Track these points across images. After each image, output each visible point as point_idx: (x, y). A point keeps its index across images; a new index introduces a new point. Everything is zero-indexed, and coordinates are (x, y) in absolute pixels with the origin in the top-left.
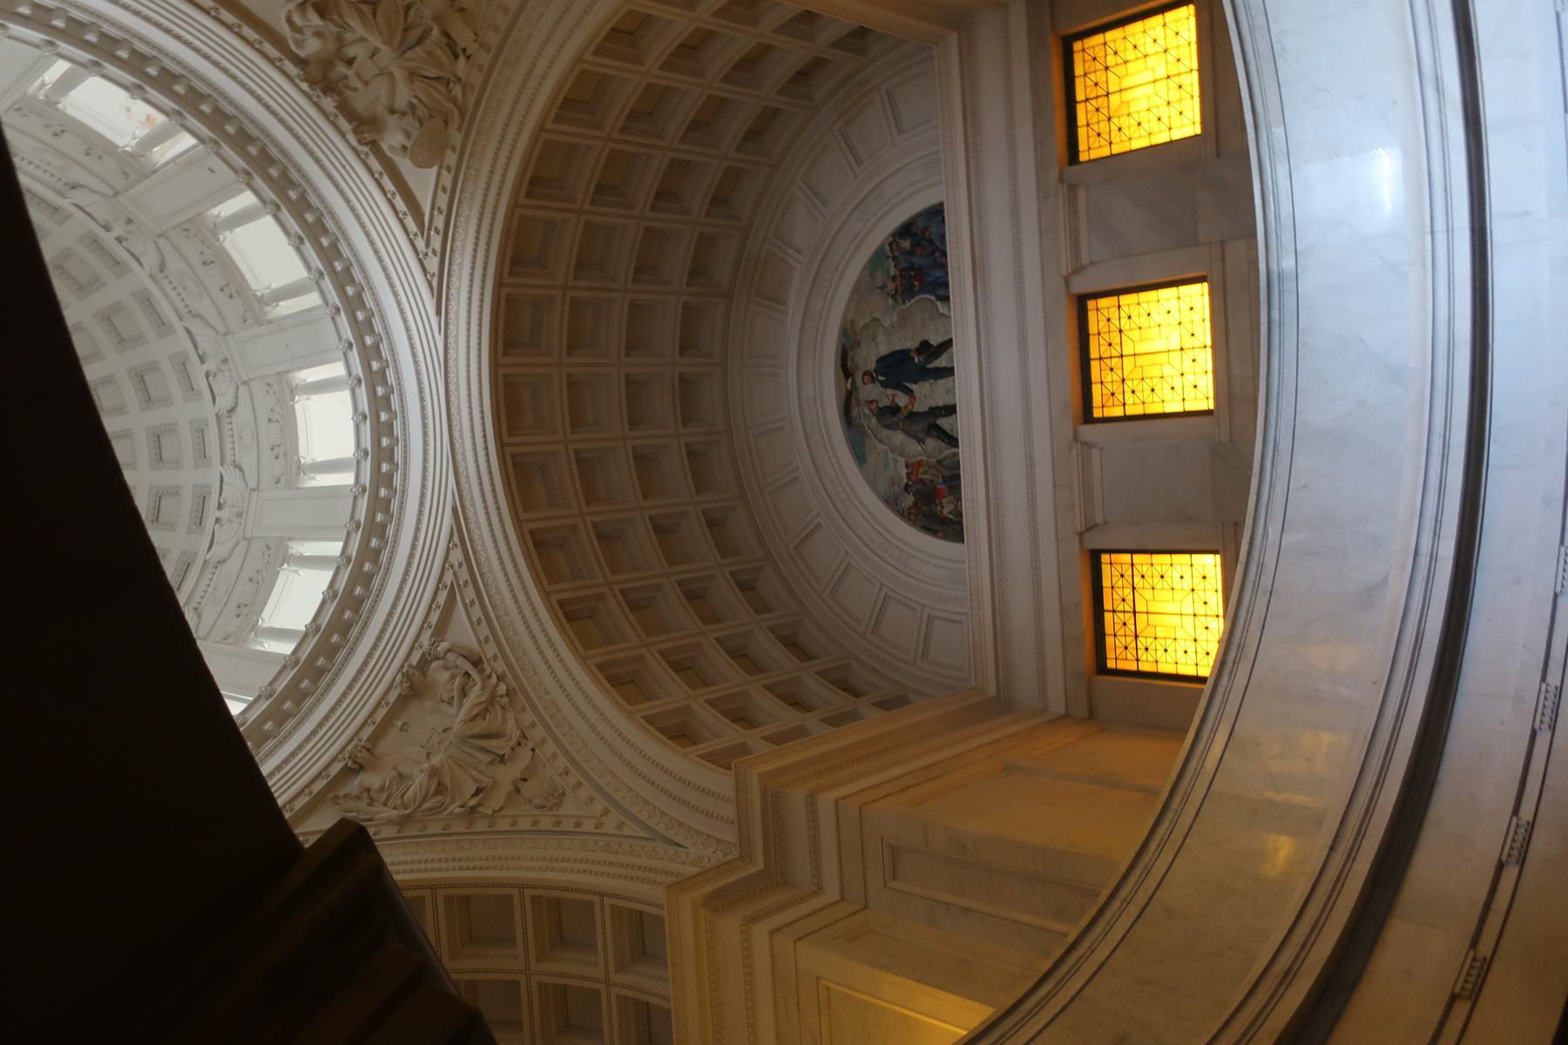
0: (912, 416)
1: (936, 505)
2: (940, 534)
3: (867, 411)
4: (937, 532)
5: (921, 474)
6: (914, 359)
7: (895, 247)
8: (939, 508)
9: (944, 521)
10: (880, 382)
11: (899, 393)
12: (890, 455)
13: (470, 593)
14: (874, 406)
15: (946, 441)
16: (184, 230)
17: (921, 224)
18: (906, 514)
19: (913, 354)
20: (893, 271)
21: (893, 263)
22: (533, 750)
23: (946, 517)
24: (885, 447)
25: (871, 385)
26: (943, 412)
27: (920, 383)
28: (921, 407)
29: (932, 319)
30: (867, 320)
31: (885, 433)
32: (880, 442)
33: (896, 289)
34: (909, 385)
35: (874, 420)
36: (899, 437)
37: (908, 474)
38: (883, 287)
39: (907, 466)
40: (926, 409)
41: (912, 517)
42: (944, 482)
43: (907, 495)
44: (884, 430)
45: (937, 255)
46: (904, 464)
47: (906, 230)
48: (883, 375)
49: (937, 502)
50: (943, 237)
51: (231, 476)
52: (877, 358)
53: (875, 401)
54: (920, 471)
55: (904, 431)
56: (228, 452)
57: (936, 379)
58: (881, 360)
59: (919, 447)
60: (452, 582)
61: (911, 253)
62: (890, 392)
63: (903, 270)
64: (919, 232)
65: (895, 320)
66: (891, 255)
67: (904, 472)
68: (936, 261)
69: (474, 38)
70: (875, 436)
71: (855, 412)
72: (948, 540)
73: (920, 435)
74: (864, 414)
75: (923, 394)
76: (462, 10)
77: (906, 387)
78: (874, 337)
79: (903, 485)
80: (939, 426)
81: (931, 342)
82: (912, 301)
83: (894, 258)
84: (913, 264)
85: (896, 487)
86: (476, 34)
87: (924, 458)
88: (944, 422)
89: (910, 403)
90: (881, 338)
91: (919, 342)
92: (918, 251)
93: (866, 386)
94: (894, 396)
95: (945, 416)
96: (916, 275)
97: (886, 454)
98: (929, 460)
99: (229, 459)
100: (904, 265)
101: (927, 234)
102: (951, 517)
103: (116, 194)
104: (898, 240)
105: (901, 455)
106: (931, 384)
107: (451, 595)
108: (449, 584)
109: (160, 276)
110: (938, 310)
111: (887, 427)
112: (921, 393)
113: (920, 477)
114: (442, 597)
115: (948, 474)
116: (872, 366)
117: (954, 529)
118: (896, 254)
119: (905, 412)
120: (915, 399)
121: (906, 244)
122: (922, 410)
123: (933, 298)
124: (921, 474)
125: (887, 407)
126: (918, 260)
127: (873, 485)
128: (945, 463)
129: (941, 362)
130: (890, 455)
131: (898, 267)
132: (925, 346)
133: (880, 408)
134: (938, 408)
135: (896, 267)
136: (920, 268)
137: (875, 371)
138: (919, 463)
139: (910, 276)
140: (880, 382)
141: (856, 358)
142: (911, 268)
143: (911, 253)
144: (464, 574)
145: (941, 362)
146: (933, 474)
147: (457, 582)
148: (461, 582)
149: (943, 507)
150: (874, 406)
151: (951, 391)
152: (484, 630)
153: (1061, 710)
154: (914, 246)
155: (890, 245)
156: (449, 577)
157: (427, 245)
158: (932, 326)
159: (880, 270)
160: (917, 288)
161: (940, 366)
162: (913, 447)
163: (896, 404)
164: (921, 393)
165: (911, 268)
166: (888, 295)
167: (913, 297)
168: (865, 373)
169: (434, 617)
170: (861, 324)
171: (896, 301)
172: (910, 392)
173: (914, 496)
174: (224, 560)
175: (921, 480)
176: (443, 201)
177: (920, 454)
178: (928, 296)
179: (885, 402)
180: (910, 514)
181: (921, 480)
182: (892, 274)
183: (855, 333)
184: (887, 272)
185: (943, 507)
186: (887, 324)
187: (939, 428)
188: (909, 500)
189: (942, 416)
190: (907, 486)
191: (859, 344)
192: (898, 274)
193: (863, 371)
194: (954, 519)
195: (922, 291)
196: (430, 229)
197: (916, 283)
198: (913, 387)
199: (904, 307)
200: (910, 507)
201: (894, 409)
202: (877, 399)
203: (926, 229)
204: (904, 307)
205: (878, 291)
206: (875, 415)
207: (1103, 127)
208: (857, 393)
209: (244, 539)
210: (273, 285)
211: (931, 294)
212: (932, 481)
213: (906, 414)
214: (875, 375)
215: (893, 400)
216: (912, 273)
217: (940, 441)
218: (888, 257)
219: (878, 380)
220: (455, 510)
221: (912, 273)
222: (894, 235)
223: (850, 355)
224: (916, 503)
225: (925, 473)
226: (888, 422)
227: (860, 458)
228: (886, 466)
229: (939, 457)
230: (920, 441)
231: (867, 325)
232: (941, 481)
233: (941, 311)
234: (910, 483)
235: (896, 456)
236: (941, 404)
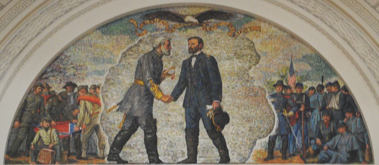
0: (150, 97)
1: (50, 121)
2: (17, 123)
4: (20, 121)
5: (85, 103)
6: (211, 103)
7: (333, 89)
8: (46, 124)
9: (31, 129)
10: (190, 60)
12: (110, 66)
14: (164, 49)
15: (118, 138)
17: (353, 124)
18: (43, 82)
19: (215, 103)
20: (308, 85)
21: (315, 86)
23: (35, 134)
24: (117, 62)
25: (187, 48)
26: (149, 136)
27: (183, 111)
30: (258, 47)
31: (134, 62)
32: (125, 55)
33: (288, 87)
34: (183, 96)
35: (149, 48)
37: (86, 87)
38: (292, 71)
39: (95, 87)
40: (155, 116)
41: (38, 90)
42: (74, 134)
43: (63, 84)
44: (136, 61)
45: (318, 141)
46: (97, 84)
48: (196, 63)
49: (53, 123)
52: (215, 58)
53: (169, 51)
54: (87, 102)
55: (134, 86)
57: (186, 130)
58: (213, 62)
59: (115, 104)
61: (323, 109)
62: (178, 71)
63: (307, 98)
64: (345, 120)
65: (255, 84)
66: (324, 84)
67: (89, 82)
68: (311, 139)
70: (130, 49)
71: (160, 24)
72: (11, 133)
73: (128, 106)
74: (154, 37)
75: (171, 113)
77: (181, 92)
78: (239, 56)
79: (74, 81)
80: (136, 130)
81: (226, 127)
82: (273, 107)
83: (321, 87)
84: (312, 110)
85: (72, 71)
88: (138, 137)
89: (164, 96)
90: (237, 64)
91: (228, 112)
92: (325, 118)
93: (186, 42)
95: (145, 139)
96: (300, 113)
97: (110, 61)
98: (100, 115)
100: (312, 99)
101: (341, 130)
102: (36, 138)
104: (339, 93)
105: (107, 80)
106: (181, 124)
110: (260, 138)
111: (140, 64)
112: (173, 110)
113: (82, 103)
115: (82, 138)
116: (208, 51)
117: (21, 142)
118: (325, 90)
120: (168, 102)
121: (334, 104)
122: (154, 110)
123: (273, 133)
124: (85, 103)
125: (162, 65)
126: (316, 116)
128: (95, 136)
129: (204, 140)
130: (110, 66)
131: (311, 92)
133: (161, 57)
134: (155, 130)
135: (312, 88)
136: (307, 119)
137: (202, 53)
138: (96, 103)
139: (299, 106)
140: (190, 60)
141: (219, 30)
142: (308, 109)
143: (323, 109)
145: (204, 140)
146: (83, 119)
149: (47, 130)
150: (164, 49)
154: (330, 113)
155: (336, 83)
158: (242, 129)
159: (310, 68)
160: (286, 114)
161: (200, 137)
163: (164, 78)
164: (173, 110)
165: (308, 109)
166: (283, 77)
167: (276, 109)
168: (201, 41)
170: (254, 40)
171: (275, 86)
172: (175, 96)
173: (60, 94)
175: (78, 104)
177: (106, 105)
178: (276, 126)
179: (167, 65)
180: (42, 86)
182: (304, 83)
183: (246, 31)
185: (47, 130)
187: (132, 130)
188: (57, 87)
189: (146, 134)
190: (74, 86)
191: (234, 36)
192: (303, 91)
193: (203, 39)
194: (32, 143)
195: (282, 117)
197: (291, 113)
198: (180, 101)
199: (267, 95)
200: (49, 88)
202: (171, 53)
203: (348, 130)
204: (267, 95)
205: (288, 64)
206: (154, 49)
208: (180, 29)
211: (276, 130)
212: (76, 118)
213: (151, 89)
214: (198, 53)
215: (168, 75)
216: (302, 109)
217: (119, 130)
218: (322, 81)
219: (192, 57)
221: (302, 109)
222: (345, 88)
223: (223, 23)
224: (52, 95)
225: (86, 108)
226: (145, 67)
228: (96, 60)
229: (101, 129)
231: (252, 47)
232: (76, 128)
233: (258, 141)
234: (76, 90)
235: (107, 73)
236: (158, 134)
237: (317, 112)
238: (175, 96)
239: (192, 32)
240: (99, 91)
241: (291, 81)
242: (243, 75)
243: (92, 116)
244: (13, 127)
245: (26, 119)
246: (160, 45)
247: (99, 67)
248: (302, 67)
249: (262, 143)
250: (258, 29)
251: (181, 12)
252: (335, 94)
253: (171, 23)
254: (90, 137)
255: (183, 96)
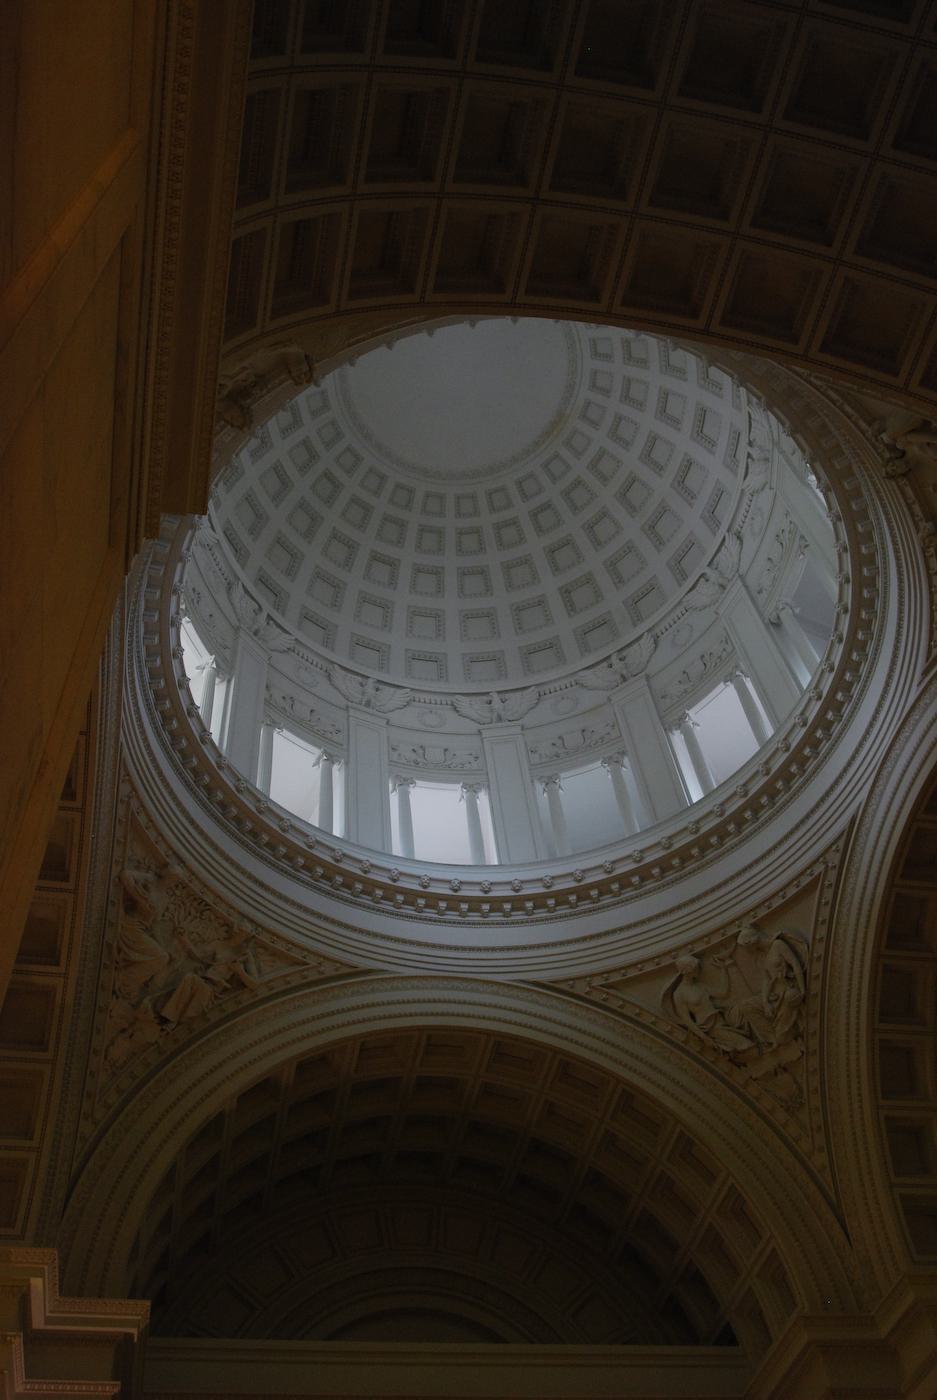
13: (296, 981)
16: (613, 726)
22: (156, 1042)
51: (399, 697)
56: (423, 696)
60: (307, 964)
69: (754, 1077)
76: (776, 1074)
86: (755, 1080)
99: (418, 696)
103: (648, 677)
107: (298, 963)
108: (308, 961)
109: (572, 680)
114: (296, 954)
144: (313, 976)
147: (308, 969)
148: (305, 973)
152: (264, 993)
156: (312, 961)
157: (593, 987)
169: (280, 946)
174: (330, 680)
176: (628, 1011)
196: (608, 993)
209: (347, 707)
210: (561, 791)
220: (369, 972)
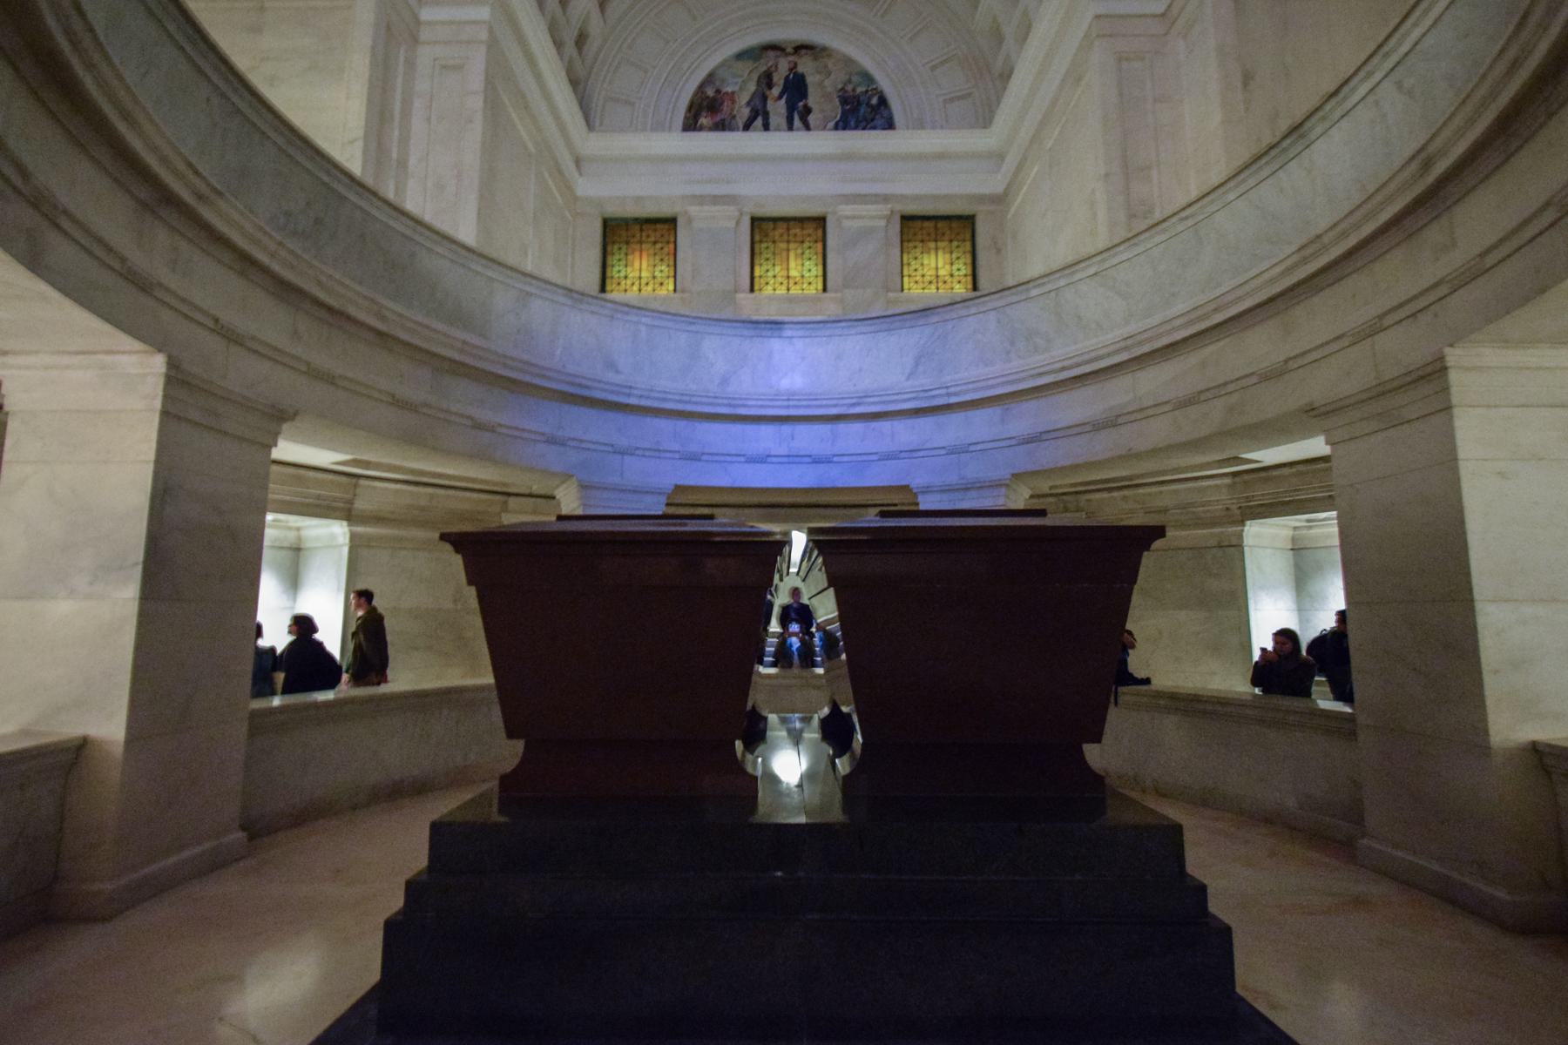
0: (765, 98)
2: (688, 115)
3: (770, 64)
9: (696, 117)
11: (781, 87)
12: (740, 80)
14: (773, 69)
17: (885, 114)
20: (860, 90)
28: (770, 105)
29: (824, 117)
31: (755, 77)
32: (751, 72)
33: (846, 91)
34: (785, 97)
35: (764, 68)
36: (752, 87)
39: (733, 93)
43: (714, 90)
47: (883, 101)
50: (874, 128)
55: (756, 90)
62: (782, 82)
63: (859, 98)
66: (870, 89)
67: (729, 89)
71: (771, 54)
74: (768, 61)
78: (819, 73)
83: (867, 91)
87: (737, 107)
88: (759, 122)
90: (818, 78)
92: (869, 110)
94: (779, 85)
97: (742, 76)
100: (861, 98)
111: (759, 78)
115: (727, 123)
116: (800, 69)
118: (870, 93)
119: (768, 93)
121: (874, 101)
126: (863, 110)
127: (722, 65)
129: (797, 122)
132: (808, 110)
138: (733, 102)
139: (853, 103)
142: (859, 104)
143: (868, 104)
145: (797, 122)
151: (778, 129)
153: (579, 192)
154: (872, 107)
155: (875, 89)
162: (744, 98)
172: (780, 97)
173: (713, 97)
181: (722, 104)
183: (823, 57)
184: (859, 85)
186: (827, 83)
188: (710, 92)
189: (763, 120)
198: (783, 101)
201: (770, 86)
203: (882, 117)
205: (847, 77)
206: (769, 69)
207: (919, 237)
212: (722, 110)
218: (868, 86)
222: (881, 92)
223: (809, 52)
224: (708, 97)
225: (727, 106)
227: (740, 56)
229: (738, 118)
230: (748, 104)
231: (826, 66)
232: (723, 117)
237: (864, 105)
238: (780, 97)
239: (791, 58)
240: (736, 95)
241: (849, 88)
242: (821, 84)
243: (732, 110)
244: (685, 117)
245: (693, 111)
246: (771, 66)
247: (735, 80)
248: (855, 79)
249: (831, 124)
250: (829, 56)
251: (783, 46)
252: (875, 94)
253: (779, 53)
254: (730, 123)
255: (785, 97)
